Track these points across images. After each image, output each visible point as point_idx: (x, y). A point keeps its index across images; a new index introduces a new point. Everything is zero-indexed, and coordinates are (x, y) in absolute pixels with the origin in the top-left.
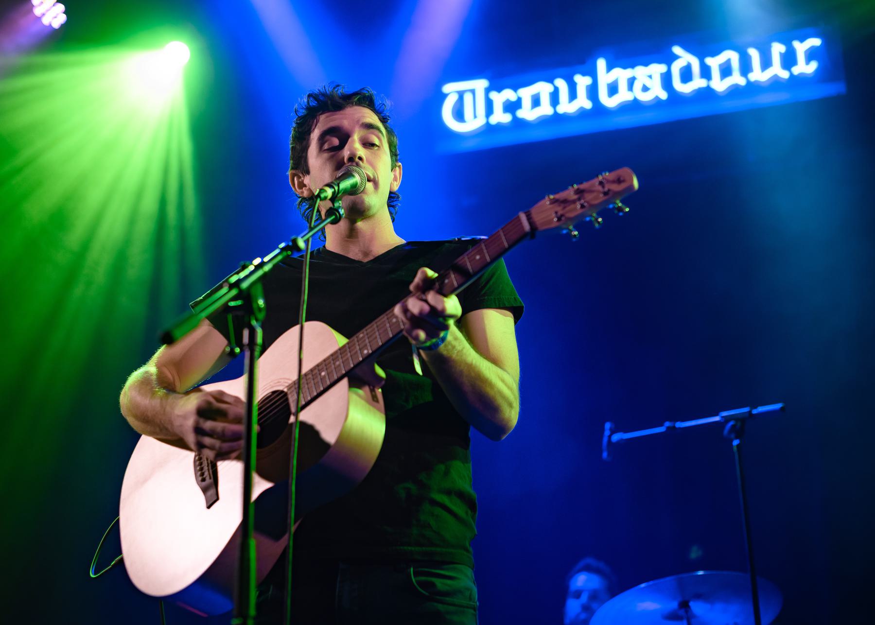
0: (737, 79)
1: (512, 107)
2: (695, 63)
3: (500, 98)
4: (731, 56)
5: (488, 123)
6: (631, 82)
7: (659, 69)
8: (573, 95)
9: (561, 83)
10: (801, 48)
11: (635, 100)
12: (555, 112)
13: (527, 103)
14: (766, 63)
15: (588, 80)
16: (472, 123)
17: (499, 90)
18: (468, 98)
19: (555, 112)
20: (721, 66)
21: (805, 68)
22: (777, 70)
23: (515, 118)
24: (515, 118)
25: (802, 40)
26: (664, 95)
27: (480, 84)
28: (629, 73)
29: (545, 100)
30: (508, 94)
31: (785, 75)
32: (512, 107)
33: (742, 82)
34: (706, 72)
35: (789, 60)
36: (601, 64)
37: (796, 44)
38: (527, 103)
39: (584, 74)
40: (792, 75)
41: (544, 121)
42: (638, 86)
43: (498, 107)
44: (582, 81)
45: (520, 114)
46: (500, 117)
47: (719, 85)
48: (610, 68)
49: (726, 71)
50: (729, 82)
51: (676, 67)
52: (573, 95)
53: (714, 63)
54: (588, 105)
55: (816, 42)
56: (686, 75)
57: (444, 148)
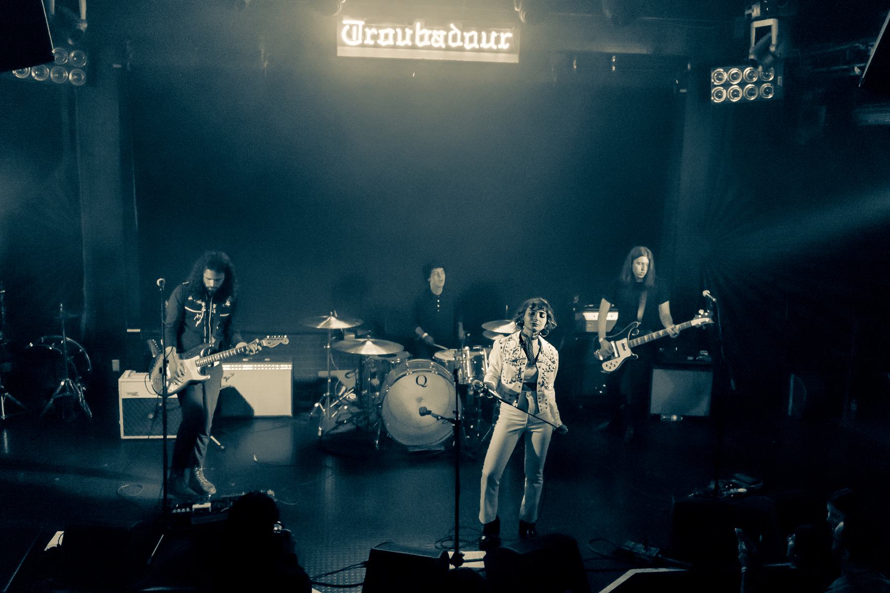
0: (475, 45)
1: (375, 37)
3: (370, 32)
4: (474, 33)
5: (363, 41)
6: (431, 36)
7: (443, 33)
8: (404, 38)
9: (399, 31)
11: (431, 45)
14: (488, 41)
15: (411, 32)
16: (356, 42)
17: (370, 27)
21: (504, 46)
22: (492, 45)
23: (376, 42)
24: (376, 42)
25: (505, 32)
26: (444, 46)
28: (430, 32)
29: (391, 37)
30: (374, 31)
31: (495, 47)
32: (375, 37)
33: (477, 46)
34: (463, 39)
35: (497, 40)
36: (418, 25)
38: (382, 37)
39: (411, 29)
42: (433, 39)
44: (409, 32)
46: (369, 41)
47: (468, 46)
48: (422, 28)
51: (451, 34)
52: (404, 38)
53: (467, 35)
54: (410, 44)
55: (509, 35)
56: (455, 39)
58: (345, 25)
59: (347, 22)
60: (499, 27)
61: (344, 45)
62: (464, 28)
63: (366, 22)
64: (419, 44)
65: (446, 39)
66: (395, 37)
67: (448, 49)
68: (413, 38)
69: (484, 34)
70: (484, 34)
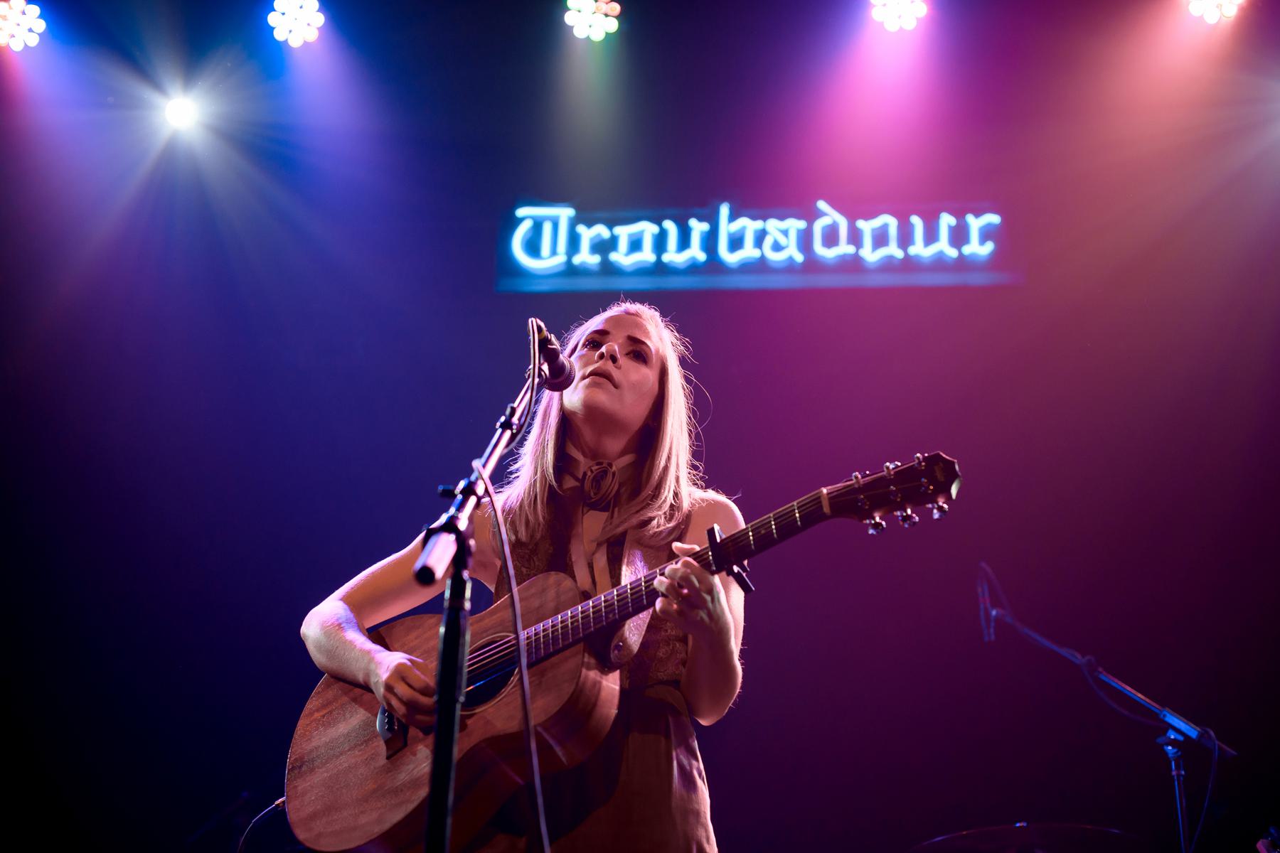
0: (893, 250)
1: (604, 247)
2: (843, 223)
3: (587, 234)
5: (569, 262)
6: (760, 238)
7: (795, 225)
8: (684, 243)
9: (670, 225)
10: (975, 223)
11: (763, 258)
12: (659, 263)
13: (623, 244)
14: (931, 237)
15: (705, 226)
16: (547, 262)
18: (547, 228)
19: (659, 263)
20: (874, 230)
21: (979, 249)
22: (943, 246)
25: (978, 214)
26: (799, 258)
27: (565, 213)
28: (759, 224)
29: (648, 243)
30: (601, 231)
31: (952, 253)
33: (899, 254)
34: (855, 238)
35: (959, 236)
36: (724, 210)
37: (970, 218)
38: (623, 244)
39: (701, 219)
40: (961, 254)
42: (768, 242)
43: (585, 245)
44: (698, 228)
45: (614, 257)
46: (586, 258)
47: (870, 255)
49: (880, 239)
50: (882, 252)
51: (819, 226)
52: (684, 243)
53: (867, 227)
54: (702, 257)
55: (993, 219)
56: (831, 238)
57: (507, 285)
58: (522, 220)
61: (517, 271)
63: (577, 208)
64: (731, 258)
65: (805, 241)
67: (812, 264)
68: (710, 242)
69: (916, 221)
70: (916, 221)
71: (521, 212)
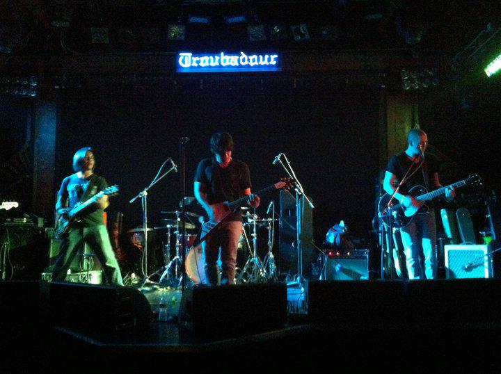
0: (256, 63)
1: (198, 62)
4: (255, 57)
7: (237, 57)
8: (214, 61)
9: (211, 57)
14: (264, 60)
15: (218, 58)
21: (273, 62)
22: (266, 62)
26: (238, 65)
30: (197, 58)
31: (268, 64)
34: (249, 60)
35: (269, 60)
36: (222, 54)
37: (271, 56)
38: (202, 61)
41: (205, 67)
44: (217, 58)
46: (195, 64)
47: (252, 64)
49: (254, 61)
51: (241, 58)
52: (214, 61)
53: (251, 58)
54: (218, 64)
55: (276, 56)
56: (244, 60)
59: (182, 54)
60: (270, 53)
61: (182, 67)
62: (249, 53)
64: (224, 65)
65: (239, 60)
66: (209, 61)
67: (240, 66)
68: (220, 61)
70: (261, 57)
71: (180, 54)
